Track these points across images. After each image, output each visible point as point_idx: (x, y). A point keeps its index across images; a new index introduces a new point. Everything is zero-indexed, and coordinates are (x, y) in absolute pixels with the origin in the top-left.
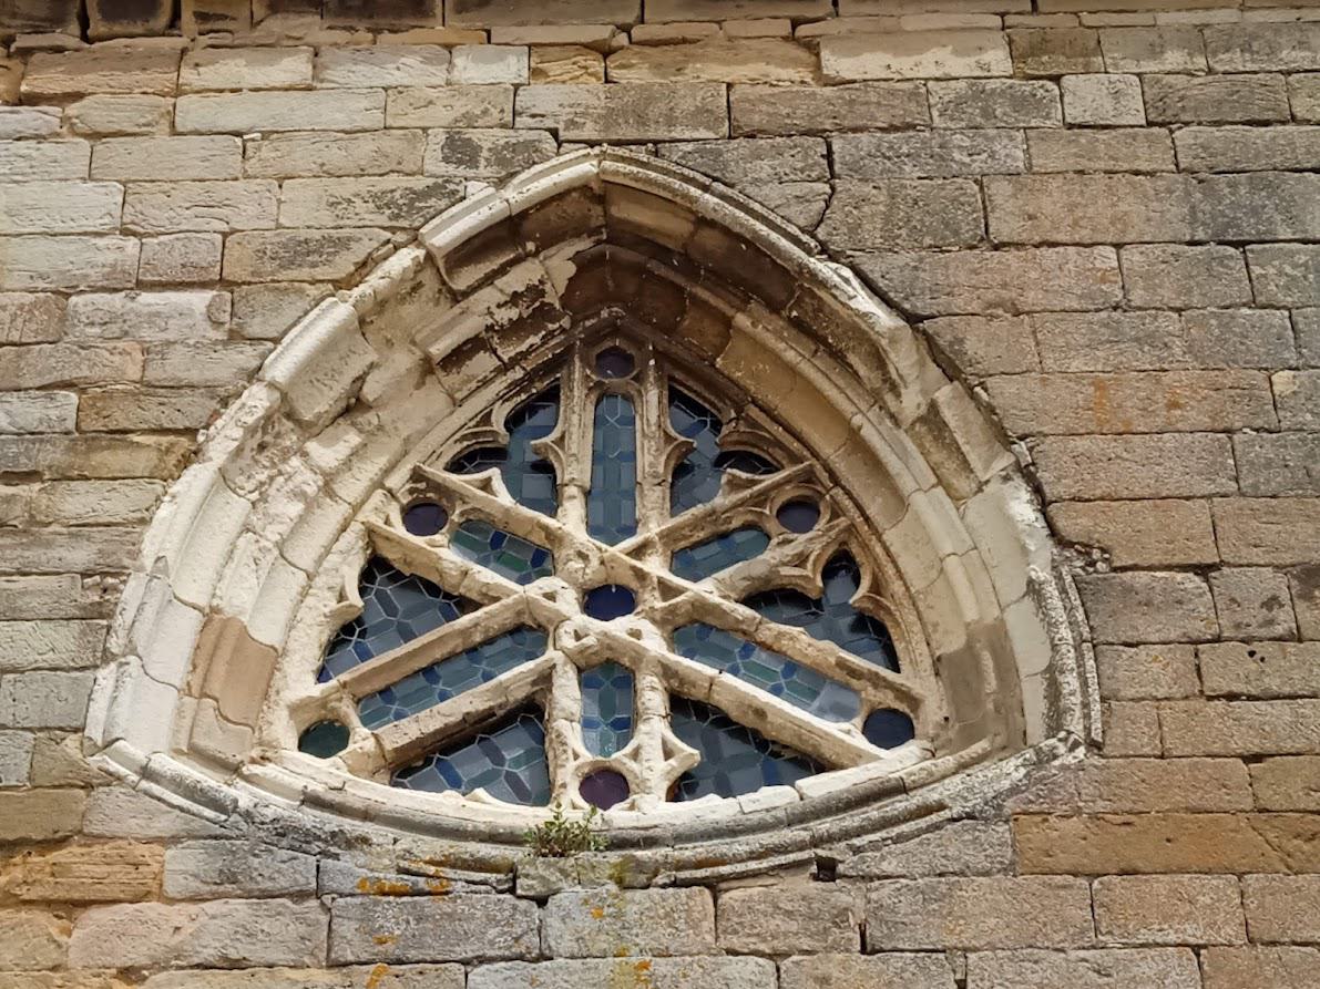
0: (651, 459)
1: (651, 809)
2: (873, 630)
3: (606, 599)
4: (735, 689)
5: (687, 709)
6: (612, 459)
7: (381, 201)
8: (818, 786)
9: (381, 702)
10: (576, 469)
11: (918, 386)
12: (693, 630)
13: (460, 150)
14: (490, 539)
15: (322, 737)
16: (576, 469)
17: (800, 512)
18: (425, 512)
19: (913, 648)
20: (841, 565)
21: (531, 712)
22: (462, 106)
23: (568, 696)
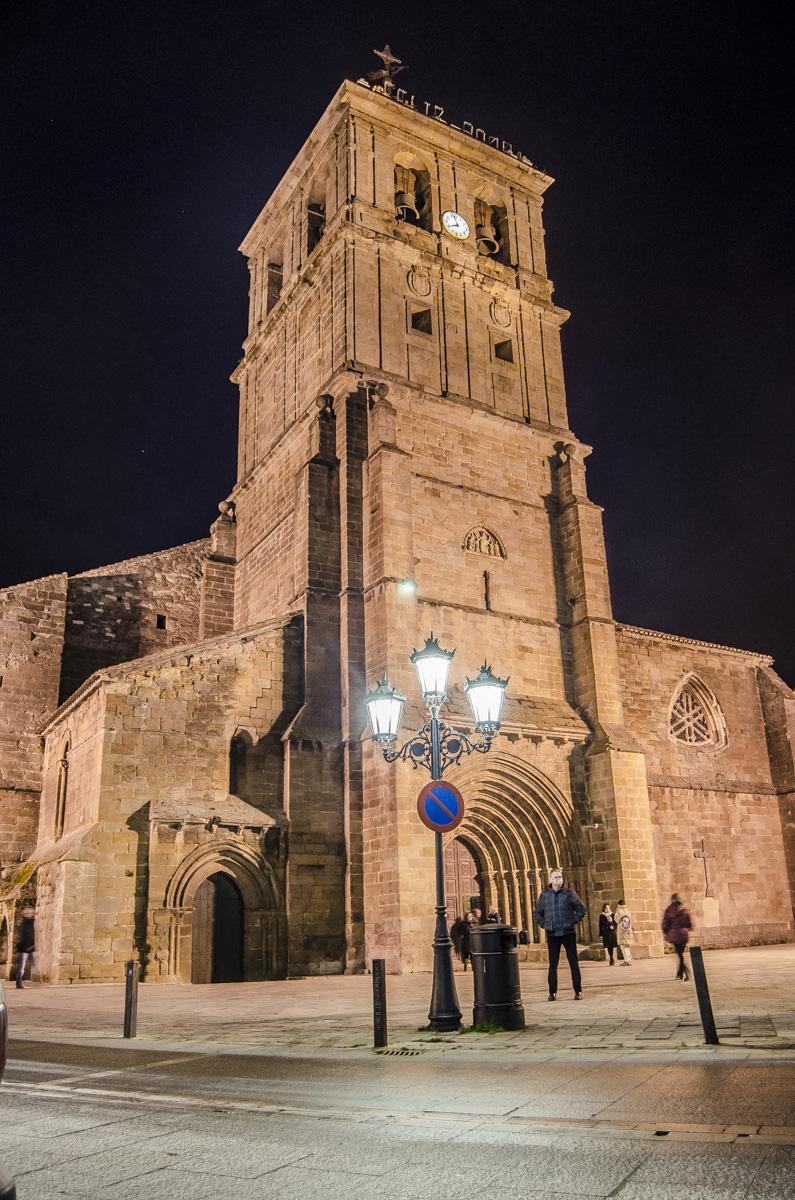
0: (690, 705)
3: (688, 720)
9: (676, 729)
10: (685, 705)
11: (715, 704)
12: (695, 725)
13: (684, 670)
16: (685, 705)
18: (675, 708)
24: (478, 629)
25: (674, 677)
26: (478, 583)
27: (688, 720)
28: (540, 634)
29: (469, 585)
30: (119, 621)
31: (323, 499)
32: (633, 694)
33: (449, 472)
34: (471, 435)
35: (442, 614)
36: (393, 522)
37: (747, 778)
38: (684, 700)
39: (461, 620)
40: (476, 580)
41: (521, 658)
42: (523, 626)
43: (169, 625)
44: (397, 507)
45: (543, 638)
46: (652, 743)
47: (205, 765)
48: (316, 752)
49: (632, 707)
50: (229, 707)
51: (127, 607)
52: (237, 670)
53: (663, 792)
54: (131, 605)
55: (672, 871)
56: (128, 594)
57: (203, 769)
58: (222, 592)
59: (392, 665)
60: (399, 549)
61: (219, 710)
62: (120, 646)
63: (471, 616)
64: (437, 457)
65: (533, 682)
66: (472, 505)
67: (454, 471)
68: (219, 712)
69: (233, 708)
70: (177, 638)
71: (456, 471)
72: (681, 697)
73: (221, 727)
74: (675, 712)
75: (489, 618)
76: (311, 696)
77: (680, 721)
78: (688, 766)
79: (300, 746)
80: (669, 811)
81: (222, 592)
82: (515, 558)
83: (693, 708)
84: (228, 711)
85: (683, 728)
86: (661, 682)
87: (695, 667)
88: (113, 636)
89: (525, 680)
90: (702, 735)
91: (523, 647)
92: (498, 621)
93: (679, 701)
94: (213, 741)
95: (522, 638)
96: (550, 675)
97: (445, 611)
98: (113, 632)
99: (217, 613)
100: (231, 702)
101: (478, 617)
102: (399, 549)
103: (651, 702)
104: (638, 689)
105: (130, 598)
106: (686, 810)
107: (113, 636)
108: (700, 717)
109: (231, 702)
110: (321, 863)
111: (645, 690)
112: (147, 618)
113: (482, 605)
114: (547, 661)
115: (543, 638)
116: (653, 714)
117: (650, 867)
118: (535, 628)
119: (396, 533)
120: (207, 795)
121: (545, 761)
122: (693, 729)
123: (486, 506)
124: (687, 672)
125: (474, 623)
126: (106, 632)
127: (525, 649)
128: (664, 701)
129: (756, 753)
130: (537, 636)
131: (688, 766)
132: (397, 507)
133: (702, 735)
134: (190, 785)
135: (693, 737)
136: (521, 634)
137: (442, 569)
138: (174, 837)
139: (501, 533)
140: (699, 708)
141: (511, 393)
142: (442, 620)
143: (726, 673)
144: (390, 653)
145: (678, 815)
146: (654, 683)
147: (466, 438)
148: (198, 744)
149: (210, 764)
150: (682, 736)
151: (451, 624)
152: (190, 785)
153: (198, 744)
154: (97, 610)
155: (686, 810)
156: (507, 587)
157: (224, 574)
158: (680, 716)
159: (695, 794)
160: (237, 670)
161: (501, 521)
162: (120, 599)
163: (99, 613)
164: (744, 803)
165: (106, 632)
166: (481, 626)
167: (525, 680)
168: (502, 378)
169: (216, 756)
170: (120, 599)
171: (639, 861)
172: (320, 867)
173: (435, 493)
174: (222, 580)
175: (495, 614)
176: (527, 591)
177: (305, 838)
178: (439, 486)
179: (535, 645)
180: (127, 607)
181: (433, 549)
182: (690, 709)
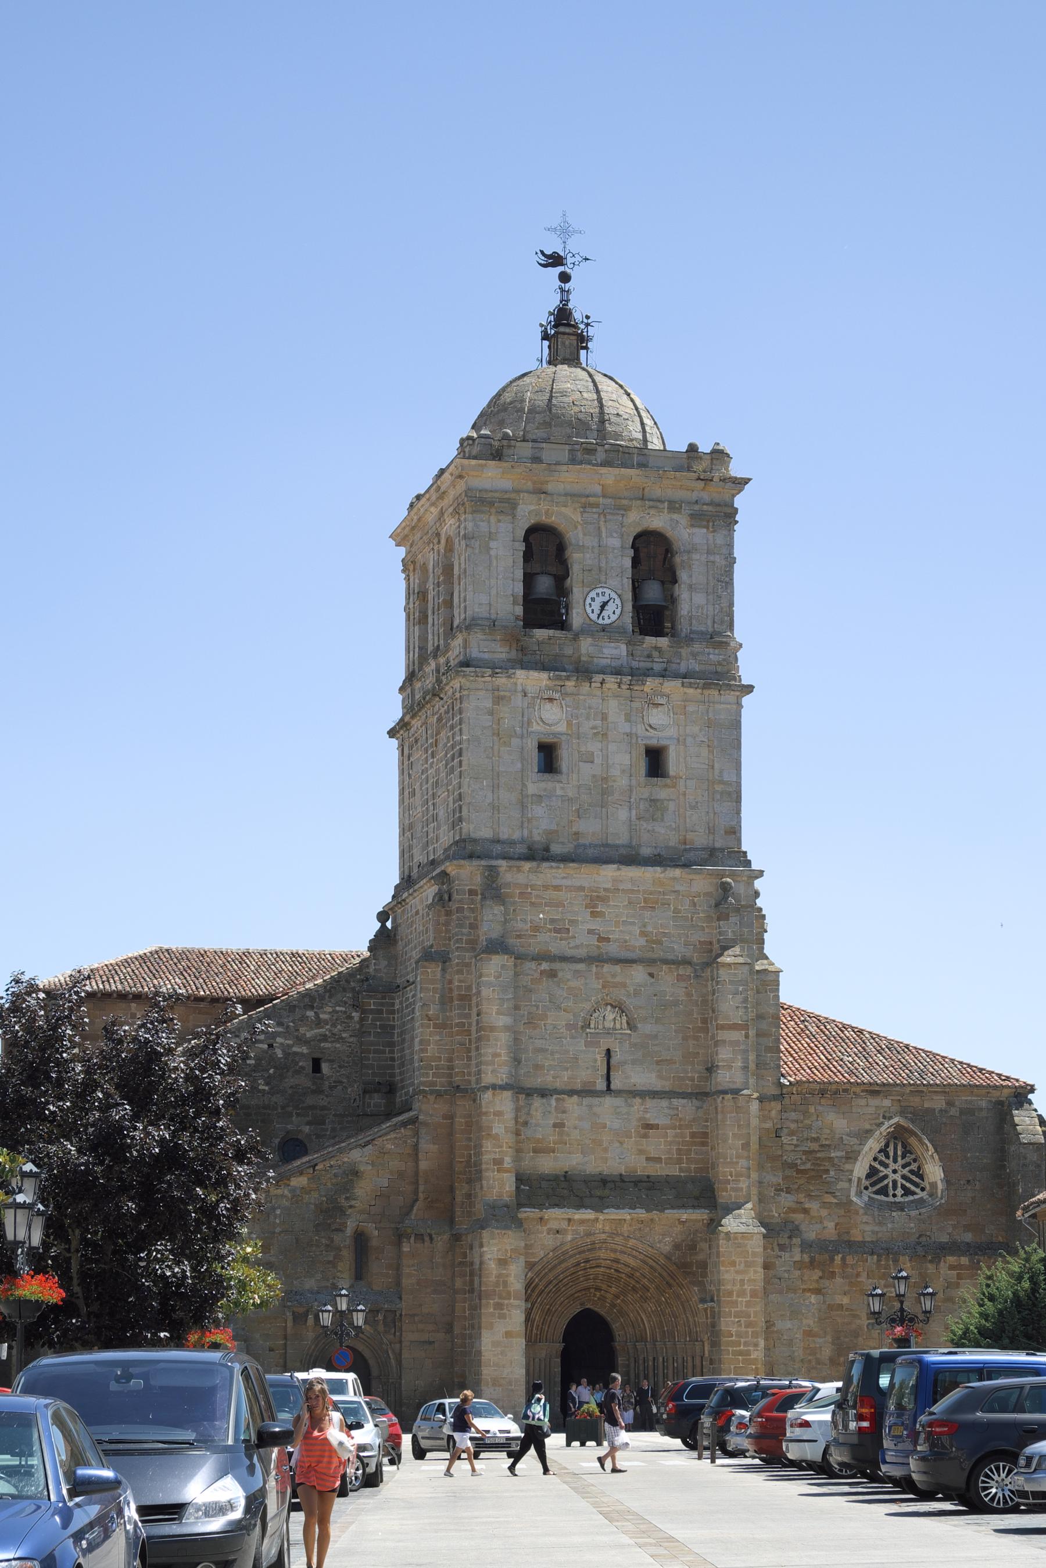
1: (899, 1199)
2: (922, 1178)
4: (908, 1185)
5: (903, 1187)
6: (895, 1153)
7: (876, 1125)
8: (916, 1197)
9: (873, 1185)
10: (891, 1154)
12: (904, 1177)
13: (884, 1117)
14: (882, 1163)
15: (866, 1188)
16: (891, 1154)
17: (915, 1160)
18: (875, 1159)
19: (926, 1179)
20: (919, 1168)
21: (887, 1185)
22: (885, 1109)
23: (891, 1185)
24: (595, 1114)
25: (867, 1127)
26: (599, 1063)
27: (894, 1173)
28: (670, 1108)
29: (587, 1068)
30: (271, 1071)
31: (437, 996)
32: (805, 1152)
33: (571, 946)
34: (603, 893)
35: (553, 1103)
36: (492, 1029)
37: (968, 1237)
38: (891, 1150)
39: (576, 1107)
40: (596, 1060)
41: (645, 1136)
42: (650, 1103)
43: (325, 1067)
44: (498, 1013)
45: (673, 1112)
46: (825, 1205)
47: (331, 1259)
48: (427, 1243)
49: (803, 1168)
50: (351, 1207)
51: (279, 1053)
52: (357, 1172)
53: (832, 1260)
54: (283, 1051)
55: (833, 1343)
56: (279, 1040)
57: (329, 1262)
58: (381, 1027)
59: (488, 1169)
60: (499, 1055)
61: (342, 1210)
62: (274, 1099)
63: (587, 1101)
64: (557, 931)
65: (658, 1160)
66: (598, 978)
67: (578, 942)
68: (342, 1211)
69: (355, 1207)
70: (335, 1082)
71: (581, 941)
72: (887, 1145)
73: (345, 1225)
74: (876, 1165)
75: (608, 1101)
76: (423, 1192)
77: (881, 1174)
78: (876, 1229)
79: (413, 1238)
80: (838, 1280)
81: (381, 1027)
82: (646, 1028)
83: (903, 1157)
84: (350, 1210)
85: (885, 1182)
86: (848, 1135)
87: (902, 1113)
88: (267, 1088)
89: (648, 1159)
90: (913, 1188)
91: (648, 1125)
92: (618, 1101)
93: (884, 1151)
94: (337, 1238)
95: (648, 1116)
96: (679, 1150)
97: (557, 1100)
98: (267, 1084)
99: (376, 1051)
100: (353, 1203)
101: (596, 1101)
102: (499, 1055)
103: (830, 1159)
104: (814, 1146)
105: (282, 1044)
106: (863, 1278)
107: (267, 1088)
108: (914, 1166)
109: (353, 1203)
110: (431, 1339)
111: (822, 1146)
112: (300, 1064)
113: (601, 1085)
114: (676, 1136)
115: (673, 1112)
116: (832, 1173)
117: (756, 1345)
118: (664, 1103)
119: (496, 1040)
120: (333, 1284)
121: (660, 1242)
122: (900, 1181)
123: (614, 976)
124: (890, 1118)
125: (590, 1107)
126: (259, 1084)
127: (649, 1126)
128: (852, 1156)
129: (989, 1206)
130: (666, 1111)
131: (876, 1229)
132: (498, 1013)
133: (913, 1188)
134: (319, 1276)
135: (899, 1192)
136: (646, 1111)
137: (557, 1056)
138: (306, 1321)
139: (630, 1003)
140: (913, 1157)
141: (662, 820)
142: (553, 1110)
143: (954, 1112)
144: (485, 1158)
145: (851, 1284)
146: (837, 1136)
147: (595, 901)
148: (324, 1241)
149: (334, 1258)
150: (884, 1191)
151: (564, 1112)
152: (319, 1276)
153: (324, 1241)
154: (248, 1062)
155: (863, 1278)
156: (634, 1062)
157: (382, 1004)
158: (882, 1169)
159: (879, 1261)
160: (357, 1172)
161: (631, 989)
162: (271, 1046)
163: (250, 1065)
164: (952, 1268)
165: (259, 1084)
166: (595, 1109)
167: (648, 1159)
168: (653, 801)
169: (341, 1251)
170: (271, 1046)
171: (742, 1340)
172: (431, 1343)
173: (552, 974)
174: (380, 1012)
175: (619, 1093)
176: (658, 1063)
177: (416, 1319)
178: (557, 966)
179: (662, 1121)
180: (279, 1053)
181: (547, 1037)
182: (899, 1159)
